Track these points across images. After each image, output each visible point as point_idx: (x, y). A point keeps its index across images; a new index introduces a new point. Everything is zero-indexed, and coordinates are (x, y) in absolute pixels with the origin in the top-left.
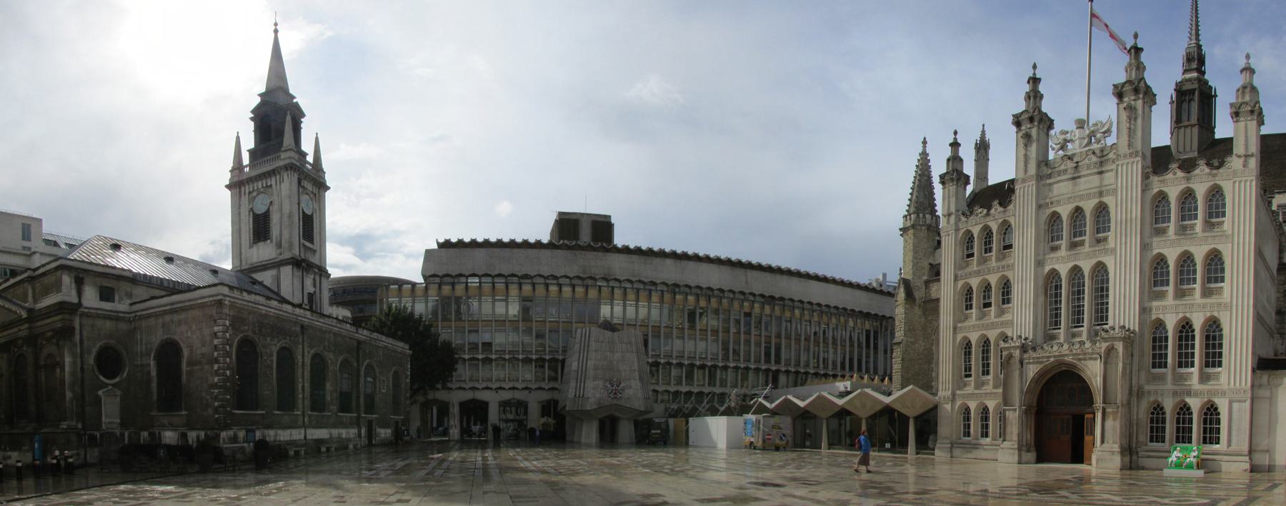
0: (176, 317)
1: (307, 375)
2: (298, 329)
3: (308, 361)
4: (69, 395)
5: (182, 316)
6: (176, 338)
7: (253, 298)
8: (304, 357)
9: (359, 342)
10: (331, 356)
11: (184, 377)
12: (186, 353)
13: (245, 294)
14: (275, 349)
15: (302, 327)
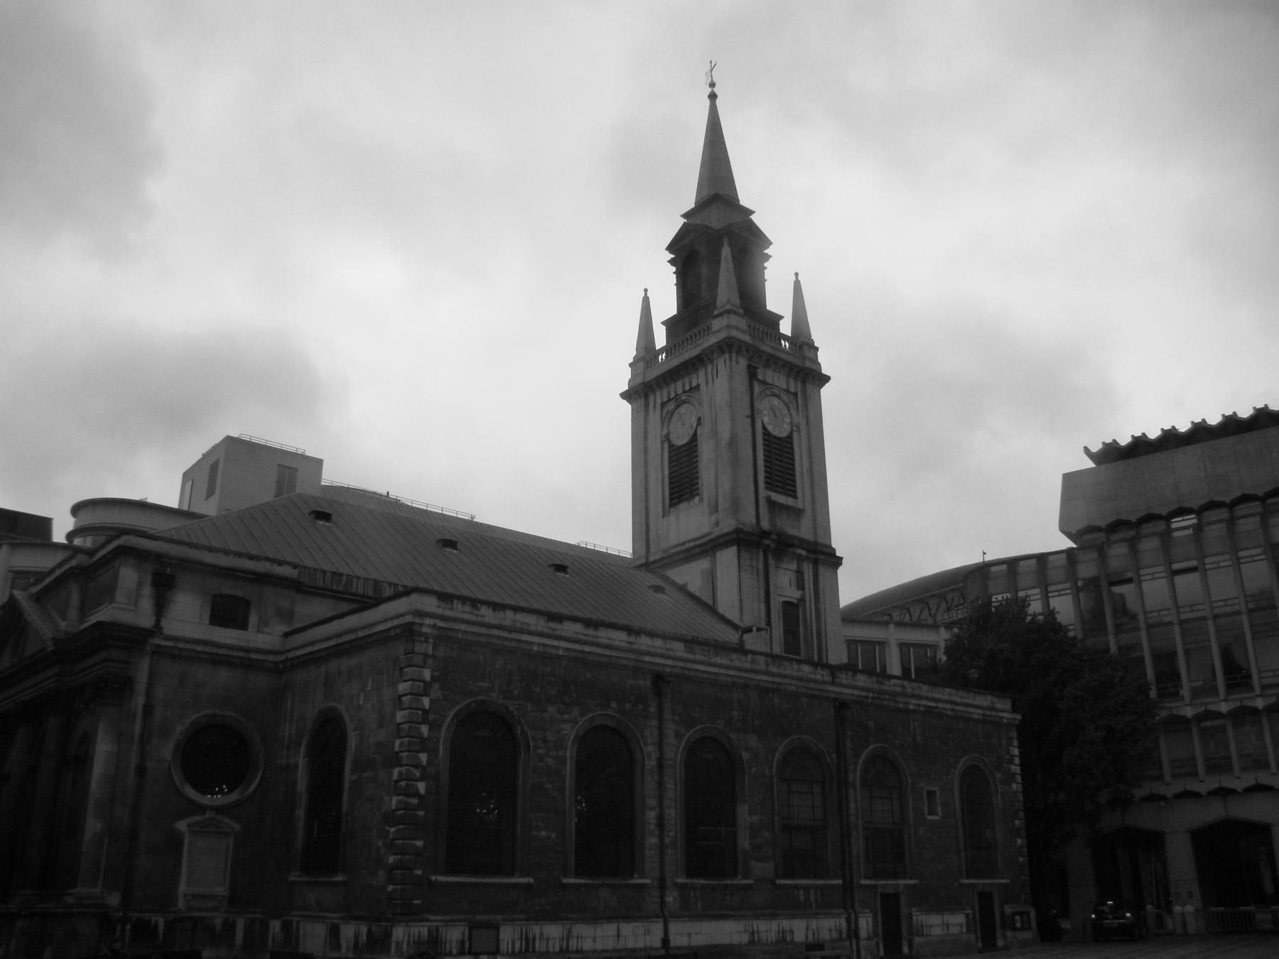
0: (346, 663)
1: (673, 790)
2: (646, 683)
3: (675, 751)
4: (93, 826)
5: (354, 661)
6: (341, 708)
7: (508, 617)
8: (662, 749)
9: (841, 706)
10: (753, 741)
11: (345, 797)
12: (352, 742)
13: (484, 610)
14: (570, 732)
15: (659, 678)
